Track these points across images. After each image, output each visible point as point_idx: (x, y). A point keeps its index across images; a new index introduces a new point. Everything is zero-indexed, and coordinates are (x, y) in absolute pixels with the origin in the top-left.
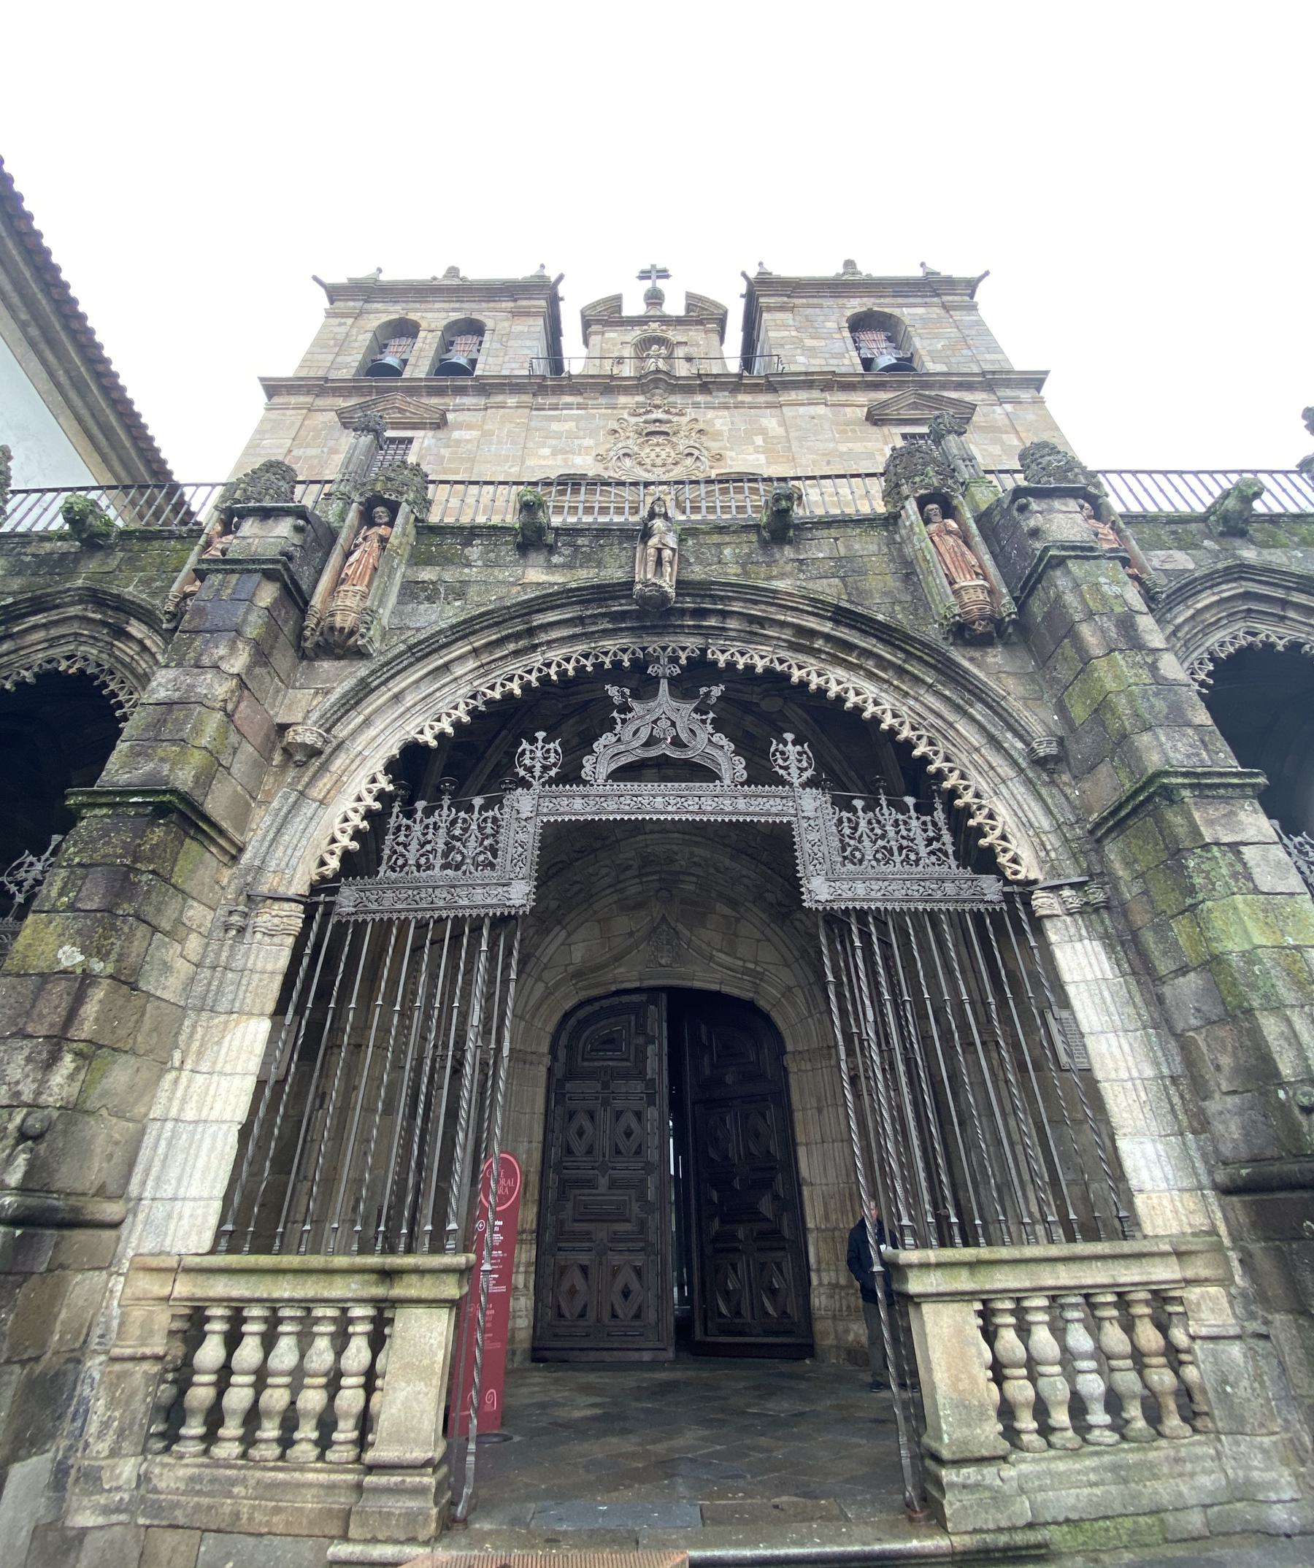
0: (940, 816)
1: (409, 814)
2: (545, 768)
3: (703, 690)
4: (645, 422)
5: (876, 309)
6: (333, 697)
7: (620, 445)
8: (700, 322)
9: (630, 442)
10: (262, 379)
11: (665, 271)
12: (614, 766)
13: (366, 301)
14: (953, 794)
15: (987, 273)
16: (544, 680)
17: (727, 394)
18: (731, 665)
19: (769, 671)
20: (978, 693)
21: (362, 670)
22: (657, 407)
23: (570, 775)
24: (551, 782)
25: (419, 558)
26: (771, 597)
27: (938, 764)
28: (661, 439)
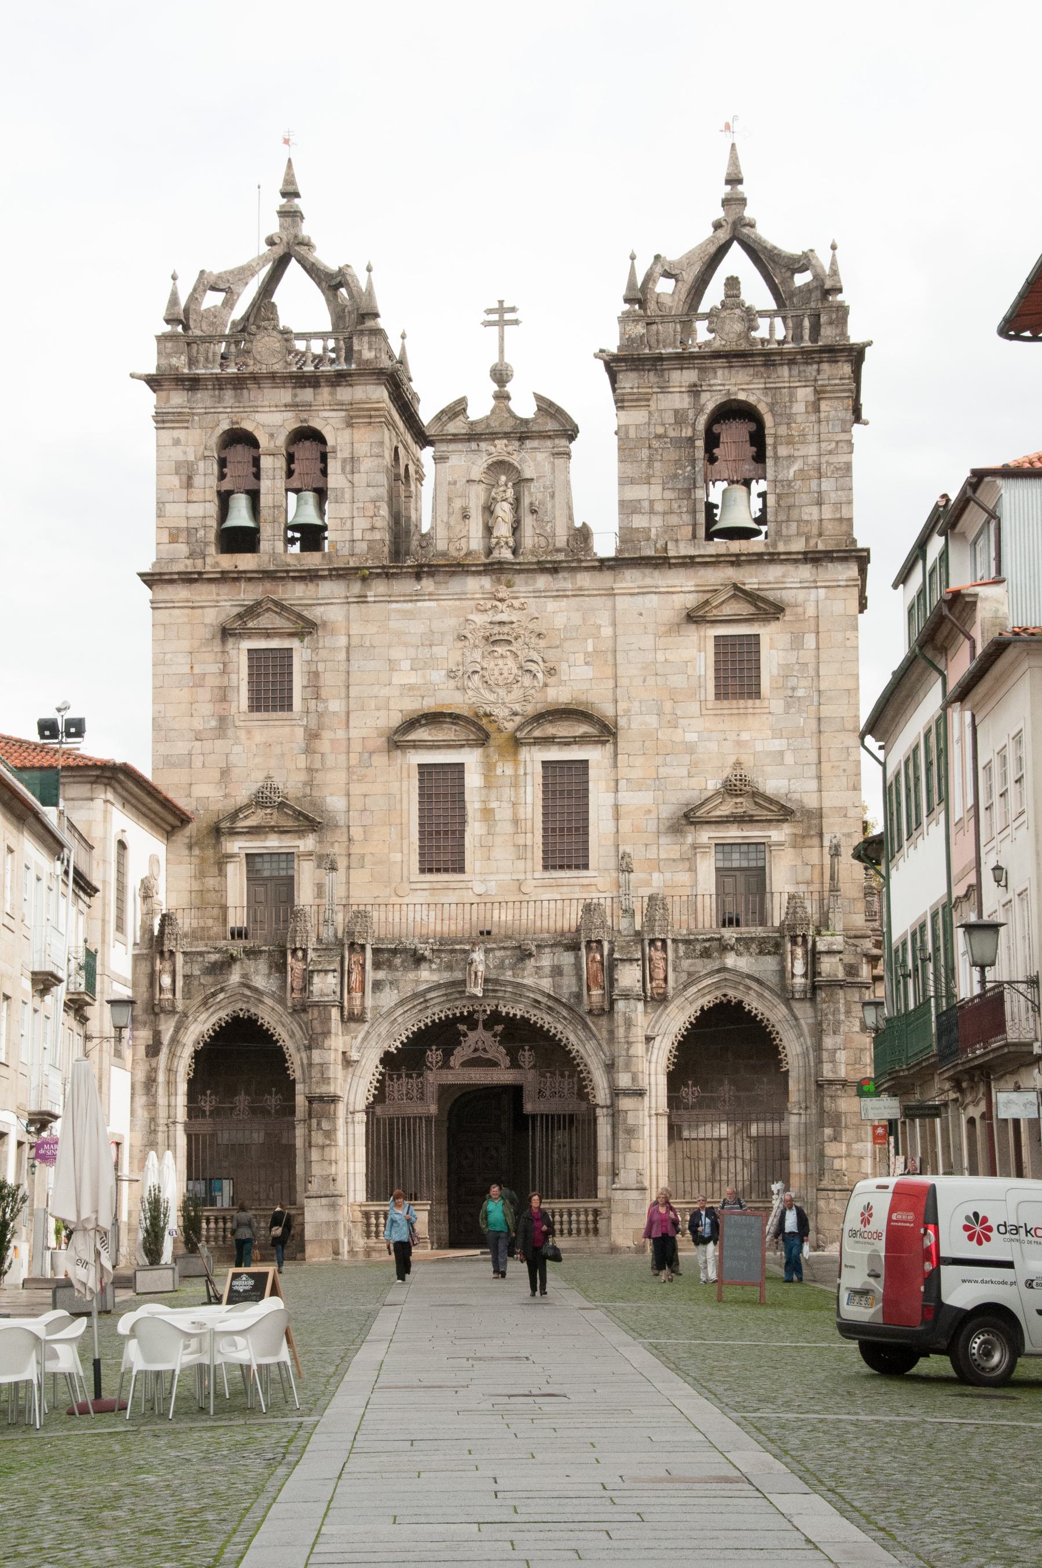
0: (575, 1079)
1: (392, 1080)
2: (437, 1062)
3: (496, 1028)
4: (491, 623)
5: (742, 396)
6: (359, 1039)
7: (469, 659)
8: (549, 437)
9: (477, 655)
10: (141, 575)
11: (513, 310)
12: (461, 1061)
13: (188, 390)
14: (581, 1072)
15: (869, 344)
16: (433, 1021)
17: (566, 575)
18: (508, 1013)
19: (522, 1017)
20: (594, 1036)
21: (366, 1027)
22: (501, 600)
23: (445, 1065)
24: (441, 1068)
25: (377, 966)
26: (524, 986)
27: (578, 1060)
28: (500, 650)
